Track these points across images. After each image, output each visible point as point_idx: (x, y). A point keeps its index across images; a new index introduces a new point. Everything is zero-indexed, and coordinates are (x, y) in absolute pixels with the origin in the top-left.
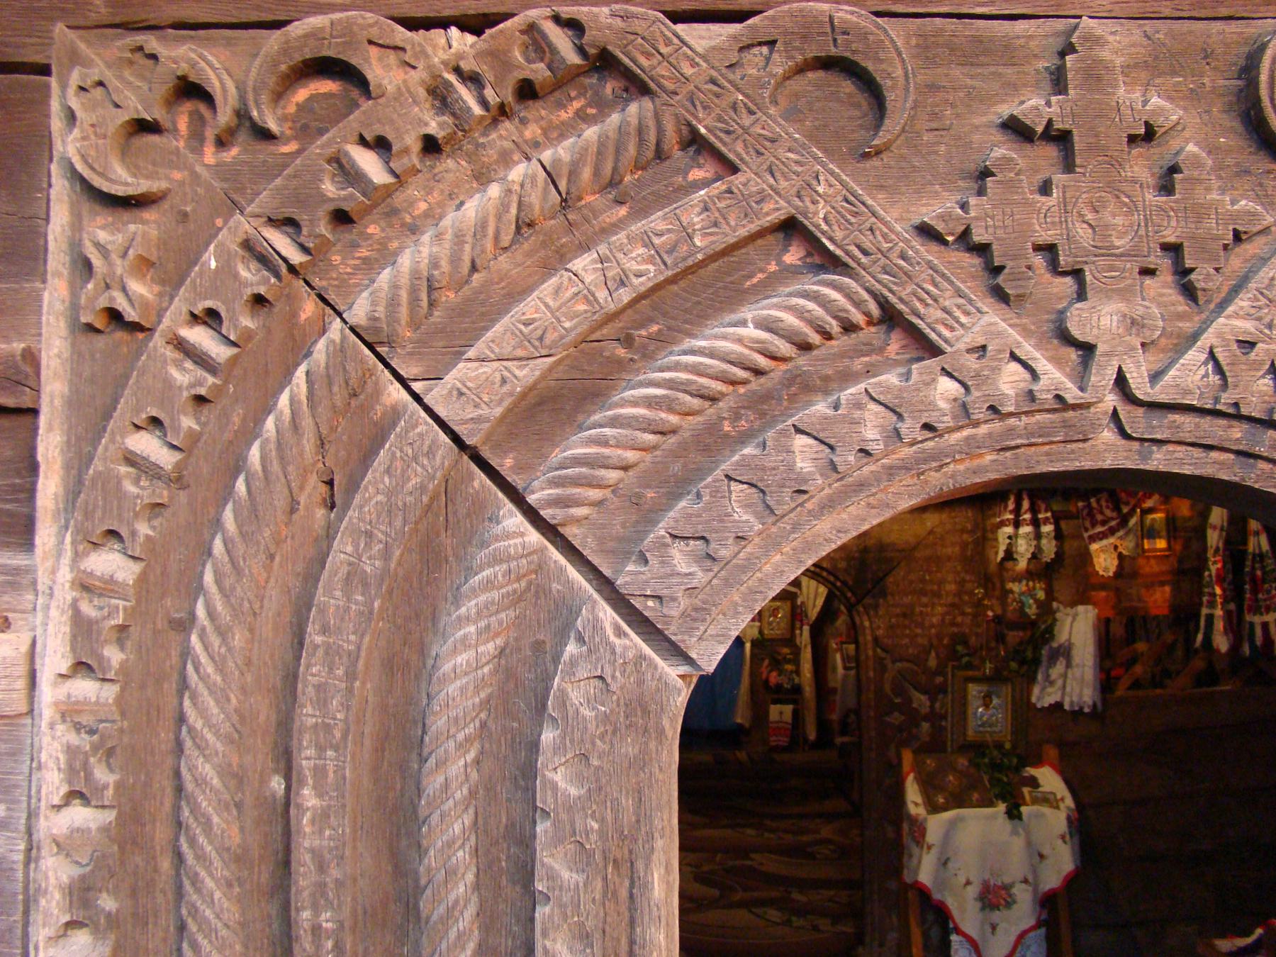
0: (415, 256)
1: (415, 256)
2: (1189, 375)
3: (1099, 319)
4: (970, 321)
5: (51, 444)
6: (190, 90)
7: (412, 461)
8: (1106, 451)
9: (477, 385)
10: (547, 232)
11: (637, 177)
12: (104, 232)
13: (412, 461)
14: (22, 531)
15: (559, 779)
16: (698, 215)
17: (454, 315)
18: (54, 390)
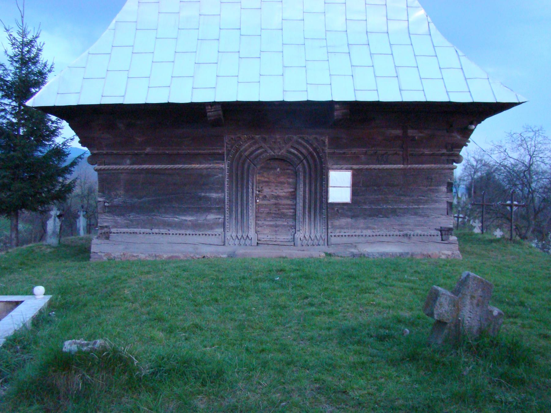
0: (244, 147)
1: (244, 147)
2: (280, 154)
3: (276, 151)
4: (269, 151)
5: (225, 156)
6: (232, 138)
7: (243, 157)
8: (276, 157)
9: (247, 153)
10: (250, 146)
11: (255, 143)
12: (228, 146)
13: (243, 157)
14: (224, 160)
15: (250, 172)
16: (257, 146)
17: (245, 150)
18: (225, 153)
